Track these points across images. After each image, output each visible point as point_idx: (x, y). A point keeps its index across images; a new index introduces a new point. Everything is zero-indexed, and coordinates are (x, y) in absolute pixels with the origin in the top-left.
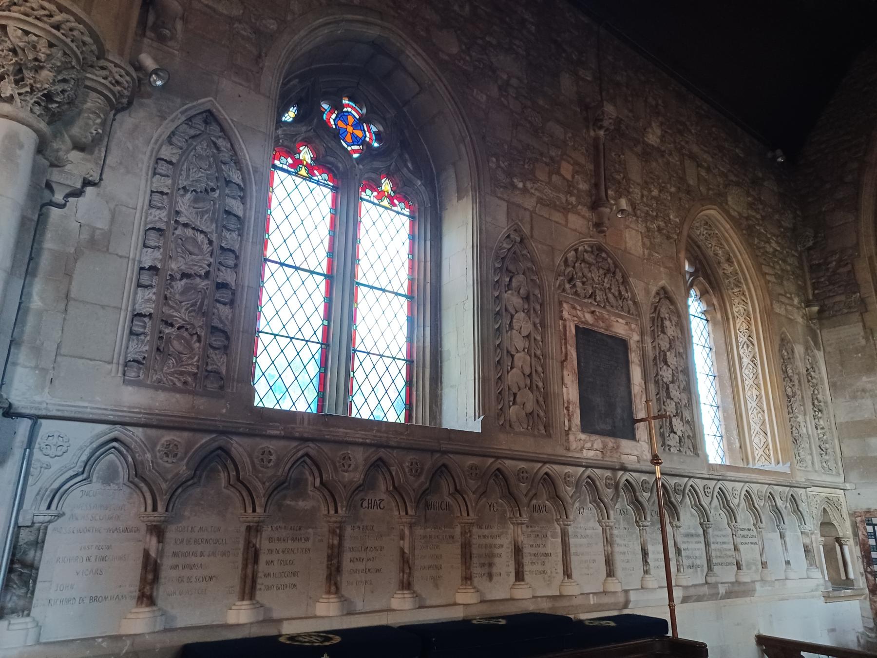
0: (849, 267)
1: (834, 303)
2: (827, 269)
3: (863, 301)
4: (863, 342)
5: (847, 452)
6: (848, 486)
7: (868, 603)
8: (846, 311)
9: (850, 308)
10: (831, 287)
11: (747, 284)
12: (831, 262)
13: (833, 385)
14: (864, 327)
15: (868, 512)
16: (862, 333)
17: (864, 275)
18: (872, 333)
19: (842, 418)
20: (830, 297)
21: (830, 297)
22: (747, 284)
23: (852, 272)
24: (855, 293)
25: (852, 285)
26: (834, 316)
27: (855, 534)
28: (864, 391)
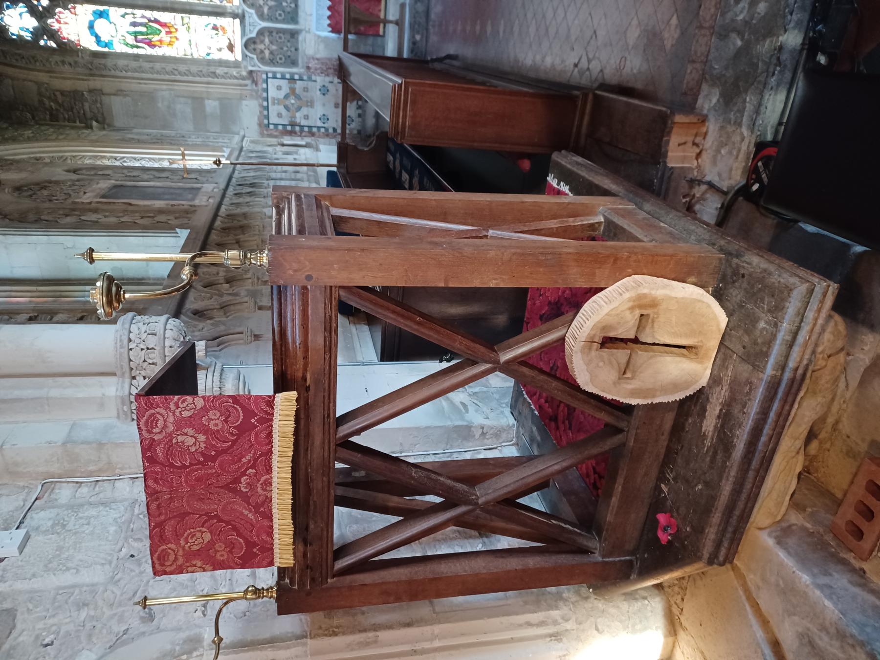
0: (57, 93)
1: (91, 111)
2: (57, 110)
3: (90, 91)
4: (128, 99)
5: (217, 129)
6: (242, 133)
7: (320, 140)
8: (99, 105)
9: (96, 101)
10: (75, 111)
11: (65, 152)
12: (51, 107)
13: (164, 127)
14: (114, 95)
15: (260, 125)
16: (121, 97)
17: (68, 85)
18: (122, 91)
19: (190, 127)
20: (84, 114)
21: (84, 114)
22: (65, 152)
23: (62, 93)
24: (83, 94)
25: (76, 95)
26: (103, 114)
27: (276, 137)
28: (169, 107)
